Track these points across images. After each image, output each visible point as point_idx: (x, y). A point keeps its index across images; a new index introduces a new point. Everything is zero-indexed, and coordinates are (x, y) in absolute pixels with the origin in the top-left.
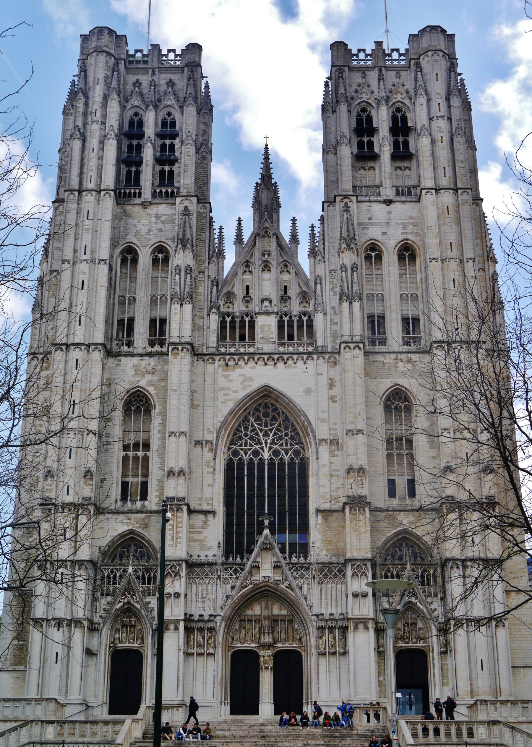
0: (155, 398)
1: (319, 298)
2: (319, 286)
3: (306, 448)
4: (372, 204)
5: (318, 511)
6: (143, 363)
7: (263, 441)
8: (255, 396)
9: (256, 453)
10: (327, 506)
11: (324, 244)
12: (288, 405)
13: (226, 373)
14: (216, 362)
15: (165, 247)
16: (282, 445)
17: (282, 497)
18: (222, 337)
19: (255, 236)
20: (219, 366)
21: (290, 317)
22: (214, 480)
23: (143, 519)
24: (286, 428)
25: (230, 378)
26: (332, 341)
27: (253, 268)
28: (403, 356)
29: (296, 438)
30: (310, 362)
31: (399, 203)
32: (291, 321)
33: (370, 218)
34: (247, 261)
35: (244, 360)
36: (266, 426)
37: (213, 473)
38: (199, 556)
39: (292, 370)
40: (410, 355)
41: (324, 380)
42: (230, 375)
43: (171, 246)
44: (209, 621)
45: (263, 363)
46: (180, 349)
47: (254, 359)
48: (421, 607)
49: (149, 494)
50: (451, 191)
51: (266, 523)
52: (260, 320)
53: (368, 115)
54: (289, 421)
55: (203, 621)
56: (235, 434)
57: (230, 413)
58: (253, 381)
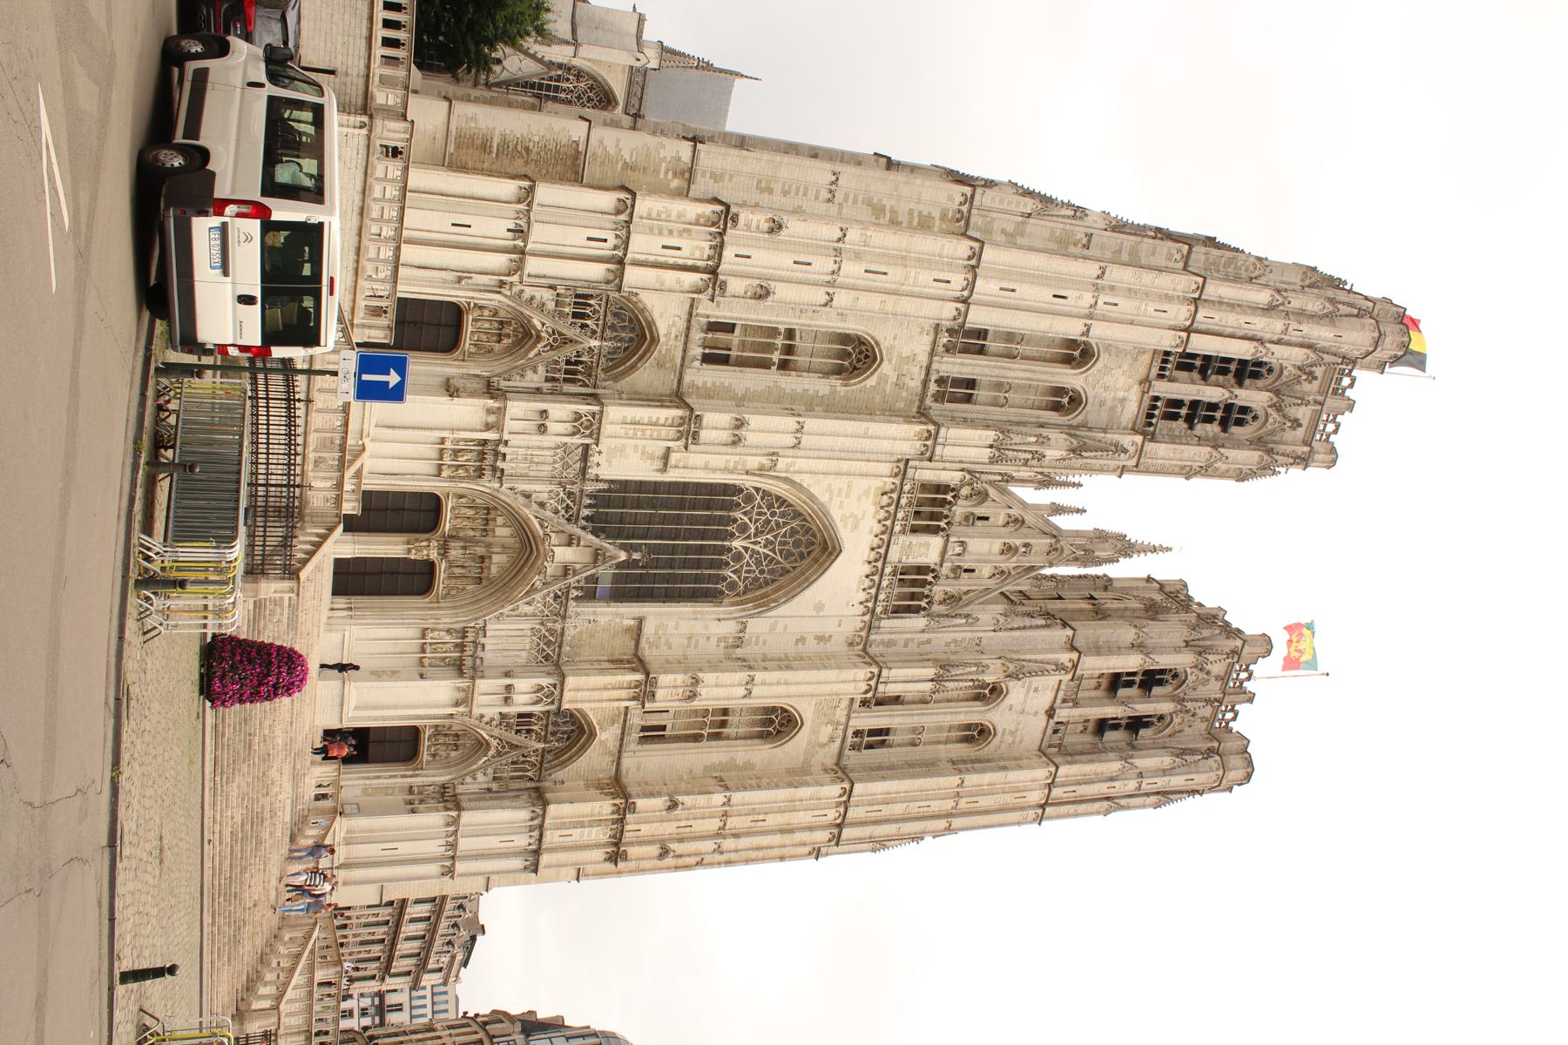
0: (859, 386)
1: (946, 622)
2: (963, 621)
3: (738, 599)
4: (1054, 693)
5: (641, 621)
6: (915, 370)
7: (759, 539)
8: (828, 532)
9: (743, 528)
10: (649, 629)
11: (1018, 628)
12: (807, 579)
13: (873, 491)
14: (891, 480)
15: (1074, 412)
16: (748, 564)
17: (670, 564)
18: (925, 487)
19: (1055, 534)
20: (885, 483)
21: (930, 583)
22: (714, 470)
23: (672, 360)
24: (771, 572)
25: (863, 498)
26: (883, 641)
27: (1012, 529)
28: (840, 733)
29: (756, 584)
30: (861, 609)
31: (1044, 725)
32: (924, 583)
33: (1036, 690)
34: (1023, 522)
35: (886, 519)
36: (781, 543)
37: (726, 470)
38: (600, 453)
39: (854, 585)
40: (839, 741)
41: (830, 628)
42: (868, 498)
43: (1075, 418)
44: (494, 469)
45: (875, 546)
46: (927, 443)
47: (883, 533)
48: (481, 762)
49: (710, 366)
50: (1043, 802)
51: (636, 556)
52: (936, 542)
53: (1167, 682)
54: (781, 575)
55: (496, 461)
56: (778, 498)
57: (812, 497)
58: (852, 531)
